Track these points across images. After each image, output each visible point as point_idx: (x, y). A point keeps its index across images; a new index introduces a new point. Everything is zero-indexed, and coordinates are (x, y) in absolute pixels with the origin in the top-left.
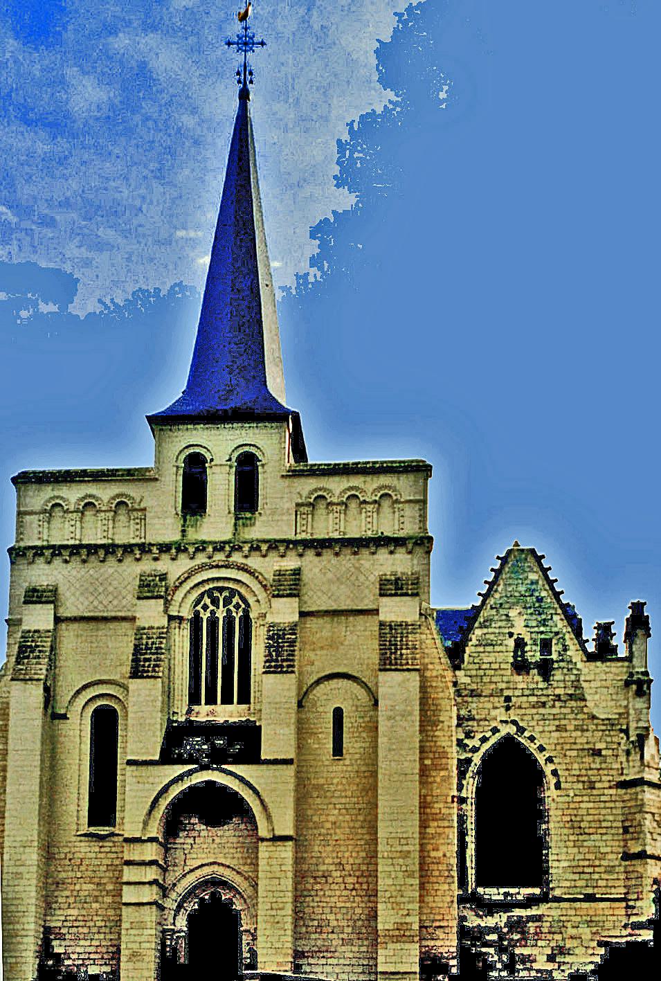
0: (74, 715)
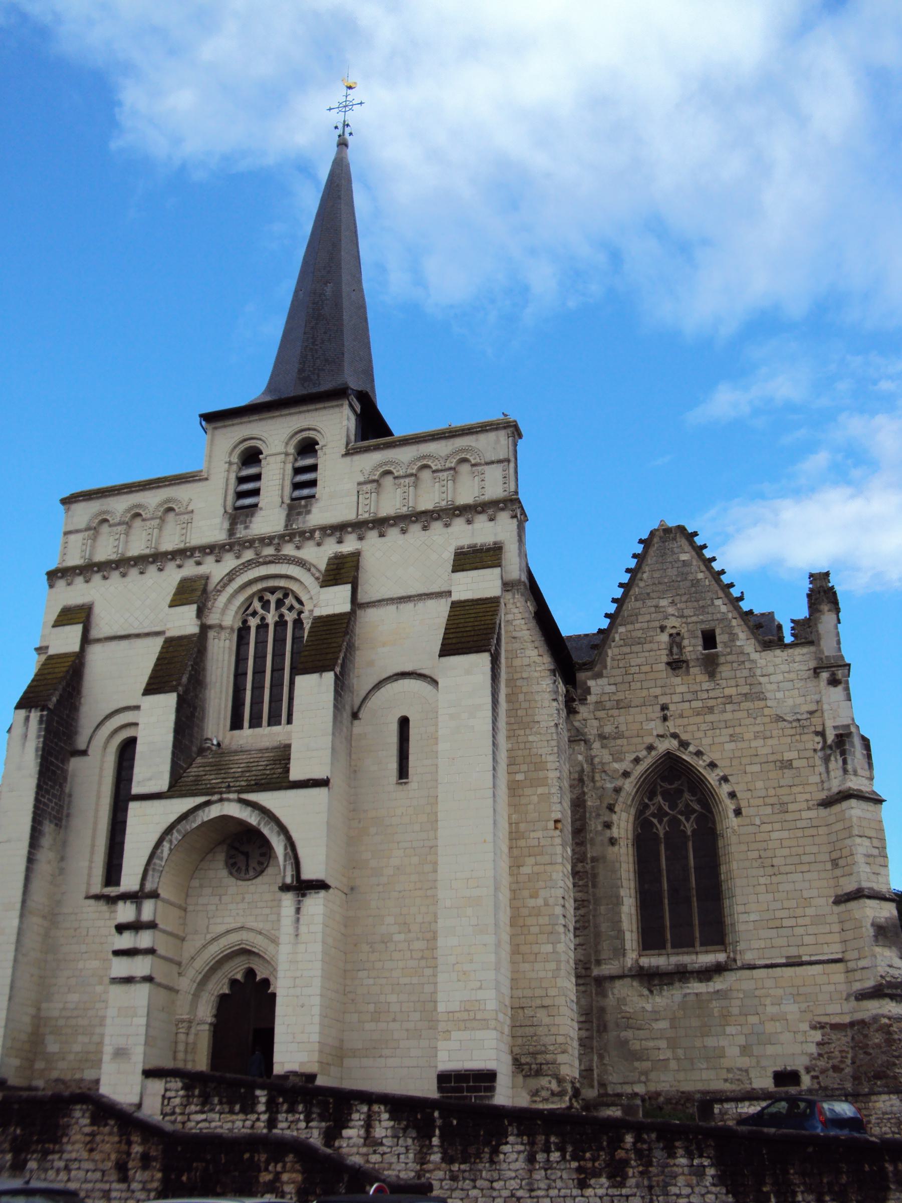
0: (95, 749)
